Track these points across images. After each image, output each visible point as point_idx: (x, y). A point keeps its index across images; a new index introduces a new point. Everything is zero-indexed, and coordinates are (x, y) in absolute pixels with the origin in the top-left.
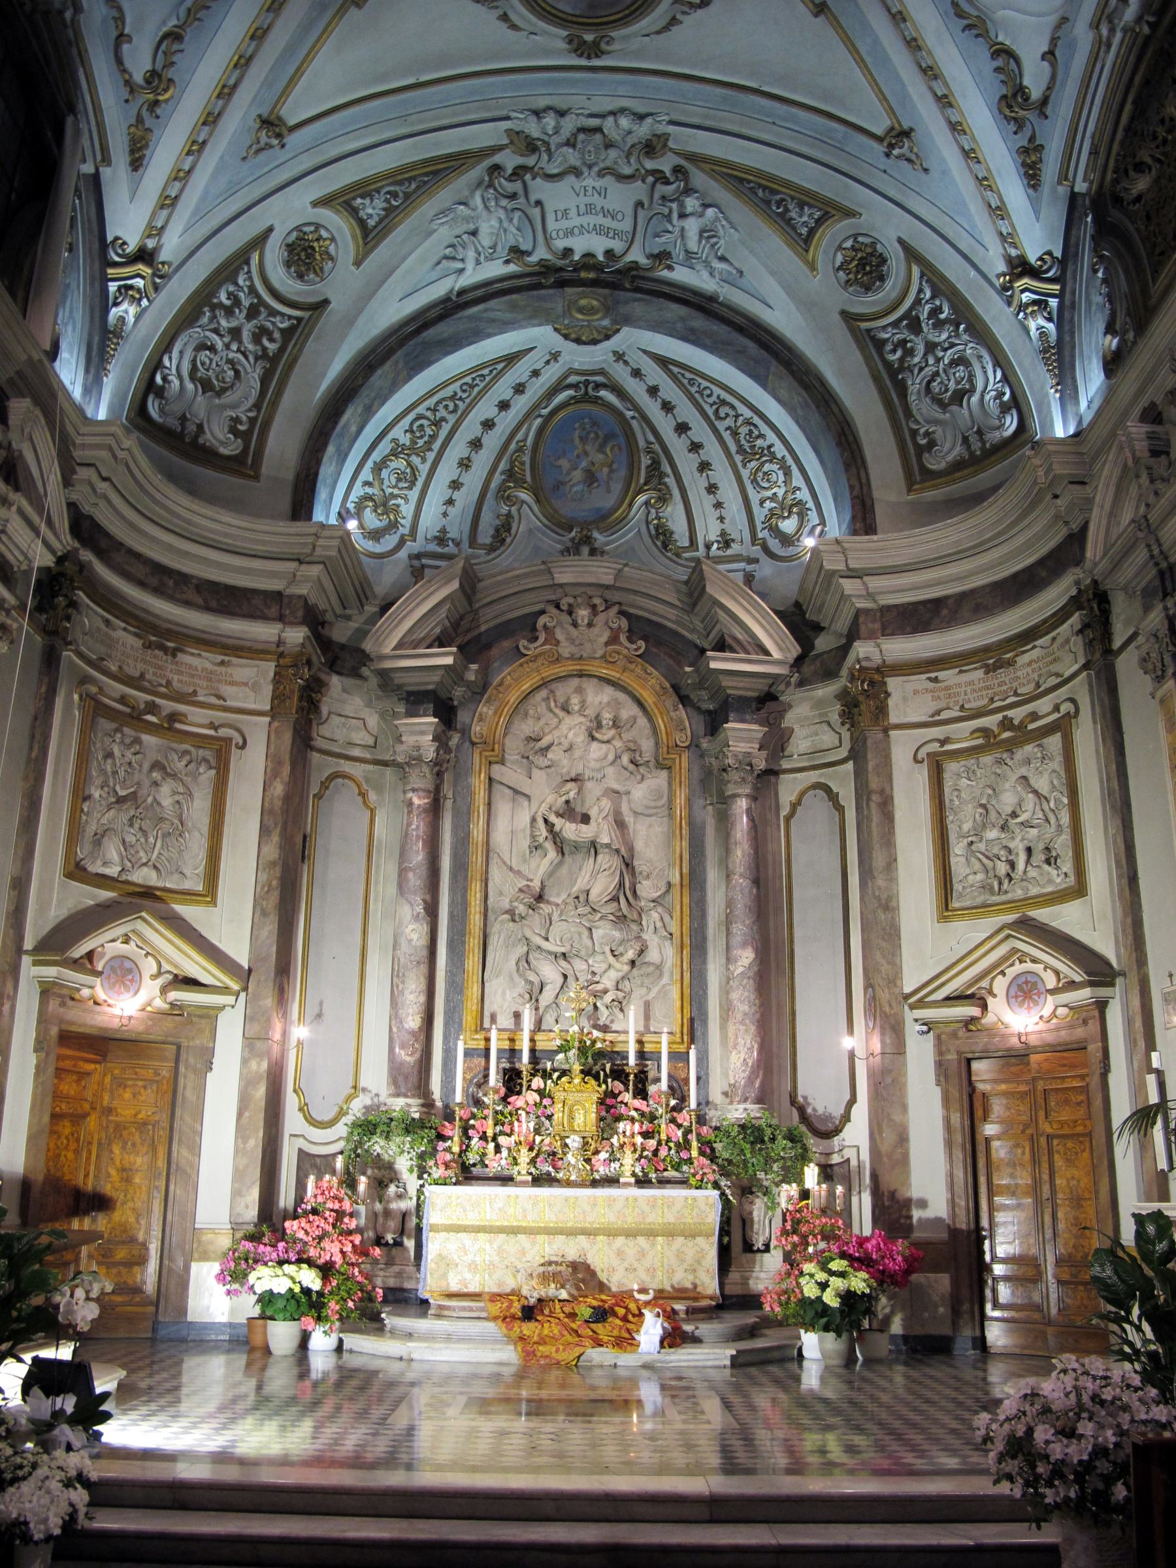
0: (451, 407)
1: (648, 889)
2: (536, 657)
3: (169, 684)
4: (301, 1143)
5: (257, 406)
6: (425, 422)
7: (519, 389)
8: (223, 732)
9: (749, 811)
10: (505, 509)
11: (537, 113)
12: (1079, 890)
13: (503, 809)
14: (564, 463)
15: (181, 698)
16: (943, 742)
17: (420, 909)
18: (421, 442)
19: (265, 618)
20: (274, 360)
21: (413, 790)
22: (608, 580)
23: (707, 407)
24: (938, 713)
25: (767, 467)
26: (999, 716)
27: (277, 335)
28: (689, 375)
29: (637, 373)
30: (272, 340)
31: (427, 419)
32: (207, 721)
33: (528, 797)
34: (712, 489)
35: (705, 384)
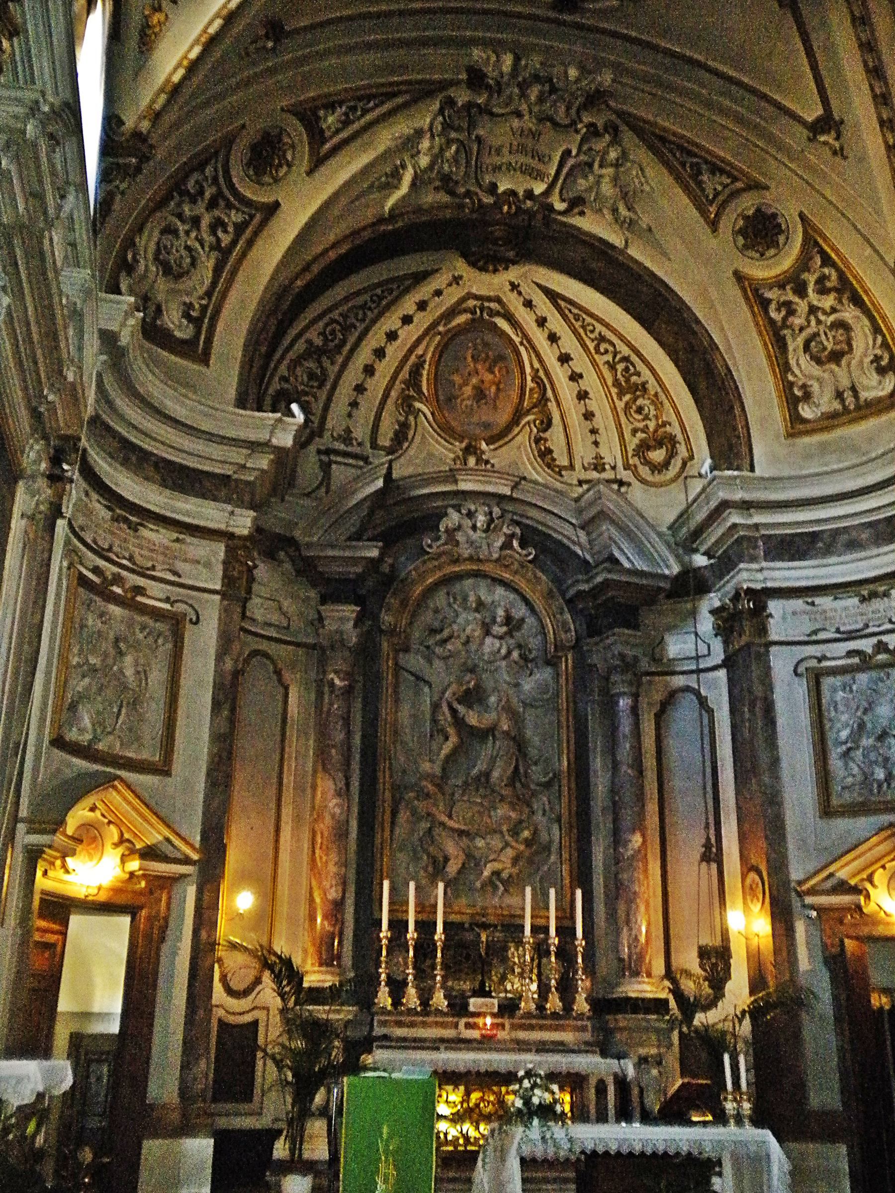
0: (360, 316)
1: (537, 774)
2: (440, 555)
3: (131, 559)
4: (221, 1013)
5: (209, 294)
6: (338, 327)
7: (422, 306)
8: (180, 607)
13: (406, 693)
16: (820, 660)
17: (341, 784)
18: (332, 345)
20: (225, 253)
21: (336, 672)
22: (507, 491)
23: (588, 342)
24: (815, 632)
25: (640, 402)
26: (874, 640)
27: (231, 229)
28: (576, 311)
29: (528, 304)
30: (226, 231)
31: (340, 324)
32: (162, 596)
33: (429, 684)
34: (588, 416)
35: (588, 320)
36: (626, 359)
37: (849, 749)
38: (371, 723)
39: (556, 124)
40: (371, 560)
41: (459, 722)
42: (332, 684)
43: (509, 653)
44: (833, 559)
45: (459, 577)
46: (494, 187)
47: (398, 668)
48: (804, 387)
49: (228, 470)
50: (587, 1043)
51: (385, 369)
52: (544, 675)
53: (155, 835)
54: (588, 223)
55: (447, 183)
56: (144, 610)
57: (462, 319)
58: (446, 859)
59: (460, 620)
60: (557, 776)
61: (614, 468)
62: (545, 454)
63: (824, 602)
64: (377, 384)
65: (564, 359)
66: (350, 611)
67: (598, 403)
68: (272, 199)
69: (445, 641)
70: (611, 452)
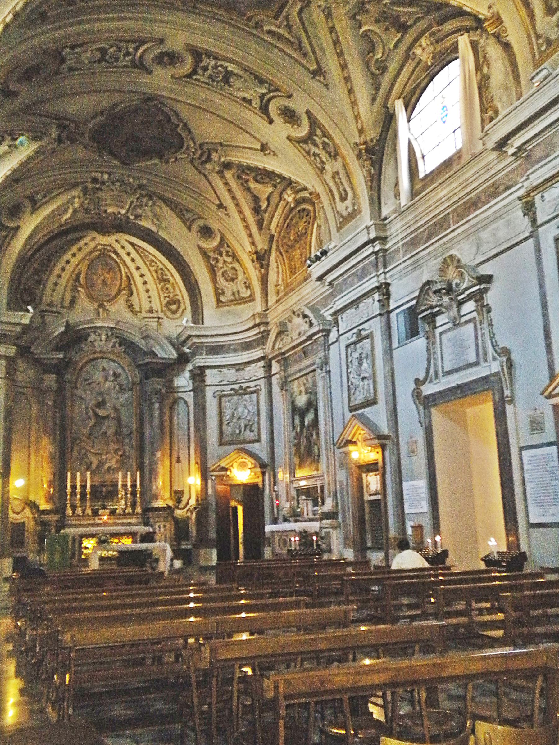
7: (80, 249)
10: (73, 294)
11: (102, 173)
12: (258, 441)
14: (95, 277)
16: (222, 391)
21: (49, 400)
22: (113, 326)
24: (221, 381)
25: (167, 286)
29: (123, 247)
34: (147, 291)
36: (161, 269)
37: (228, 423)
38: (63, 417)
39: (127, 193)
40: (61, 359)
41: (96, 415)
42: (47, 404)
43: (115, 387)
44: (229, 355)
46: (105, 211)
47: (73, 395)
48: (222, 289)
50: (140, 523)
51: (66, 276)
52: (128, 395)
54: (143, 223)
55: (87, 211)
57: (97, 253)
58: (91, 463)
59: (96, 376)
60: (131, 433)
61: (157, 312)
62: (131, 306)
63: (225, 370)
64: (63, 282)
66: (53, 377)
67: (151, 285)
68: (15, 225)
69: (90, 384)
70: (156, 305)
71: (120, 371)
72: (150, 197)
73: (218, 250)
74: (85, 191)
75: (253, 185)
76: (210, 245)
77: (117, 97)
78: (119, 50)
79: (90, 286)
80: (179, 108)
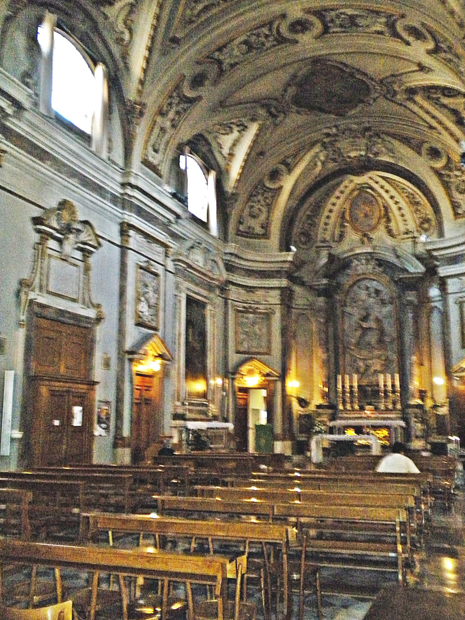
1: (387, 339)
9: (414, 318)
13: (346, 319)
15: (258, 303)
19: (276, 277)
22: (372, 251)
41: (361, 327)
45: (359, 281)
46: (349, 157)
47: (343, 312)
48: (458, 203)
49: (280, 269)
52: (389, 308)
53: (267, 370)
55: (334, 160)
56: (260, 313)
57: (356, 193)
62: (390, 232)
65: (392, 197)
66: (321, 299)
70: (412, 226)
71: (380, 288)
72: (378, 135)
73: (447, 167)
74: (324, 145)
75: (445, 101)
76: (439, 164)
77: (291, 70)
78: (258, 35)
79: (354, 220)
80: (343, 59)
